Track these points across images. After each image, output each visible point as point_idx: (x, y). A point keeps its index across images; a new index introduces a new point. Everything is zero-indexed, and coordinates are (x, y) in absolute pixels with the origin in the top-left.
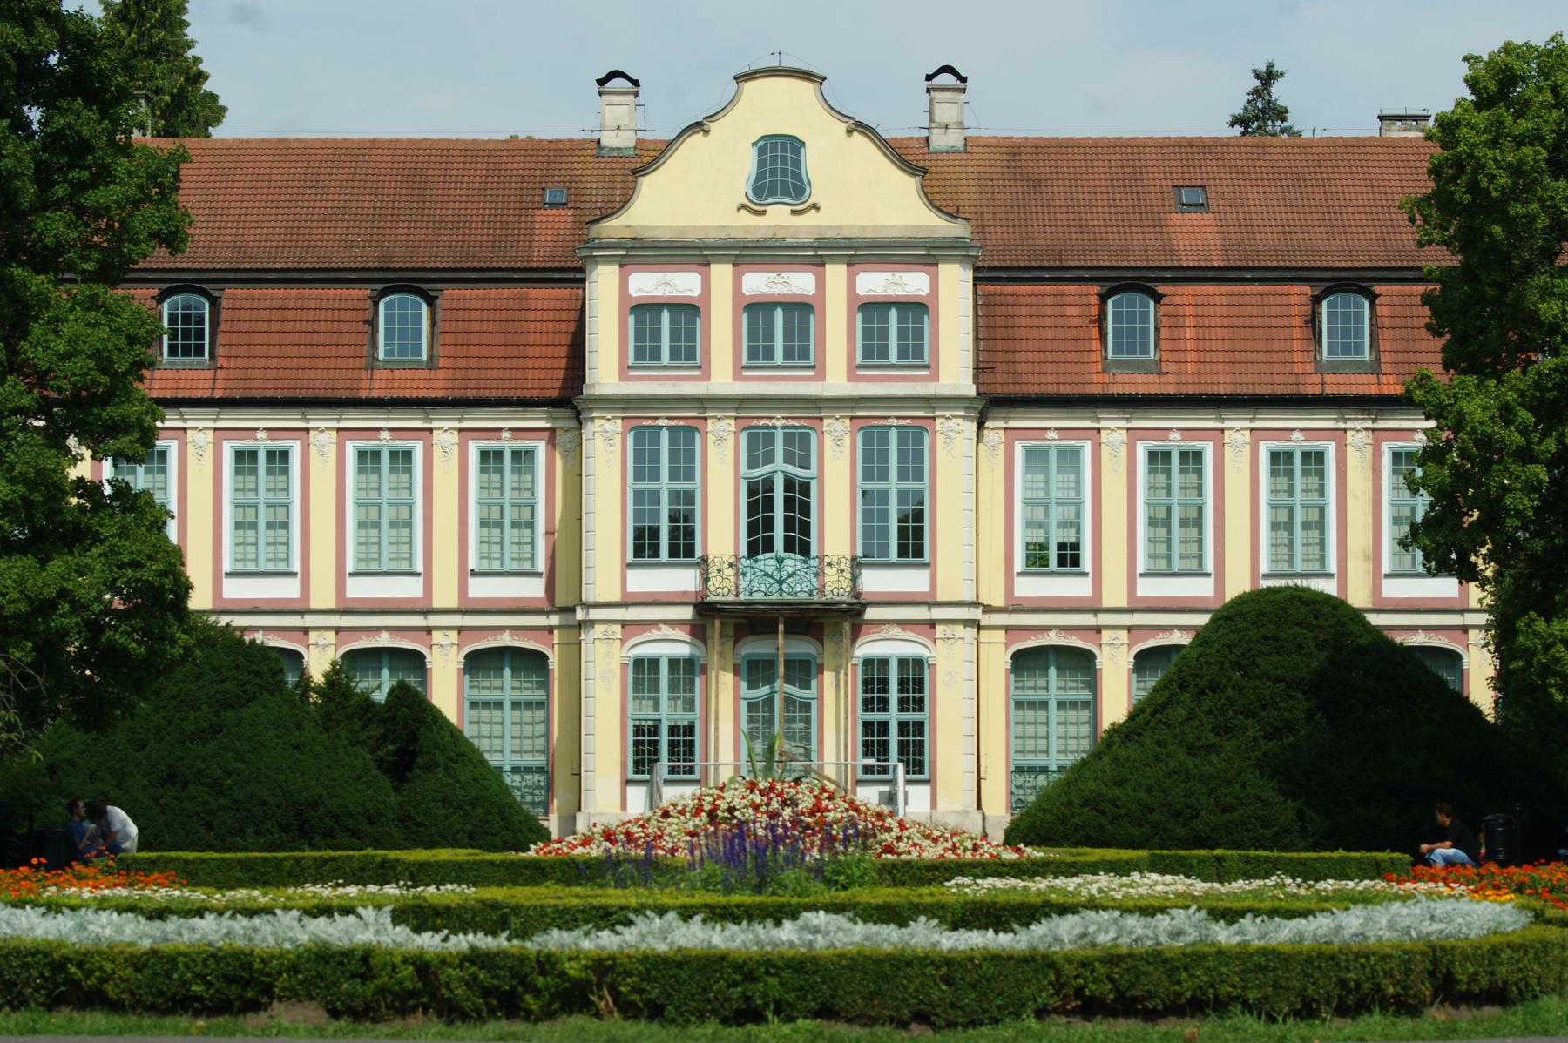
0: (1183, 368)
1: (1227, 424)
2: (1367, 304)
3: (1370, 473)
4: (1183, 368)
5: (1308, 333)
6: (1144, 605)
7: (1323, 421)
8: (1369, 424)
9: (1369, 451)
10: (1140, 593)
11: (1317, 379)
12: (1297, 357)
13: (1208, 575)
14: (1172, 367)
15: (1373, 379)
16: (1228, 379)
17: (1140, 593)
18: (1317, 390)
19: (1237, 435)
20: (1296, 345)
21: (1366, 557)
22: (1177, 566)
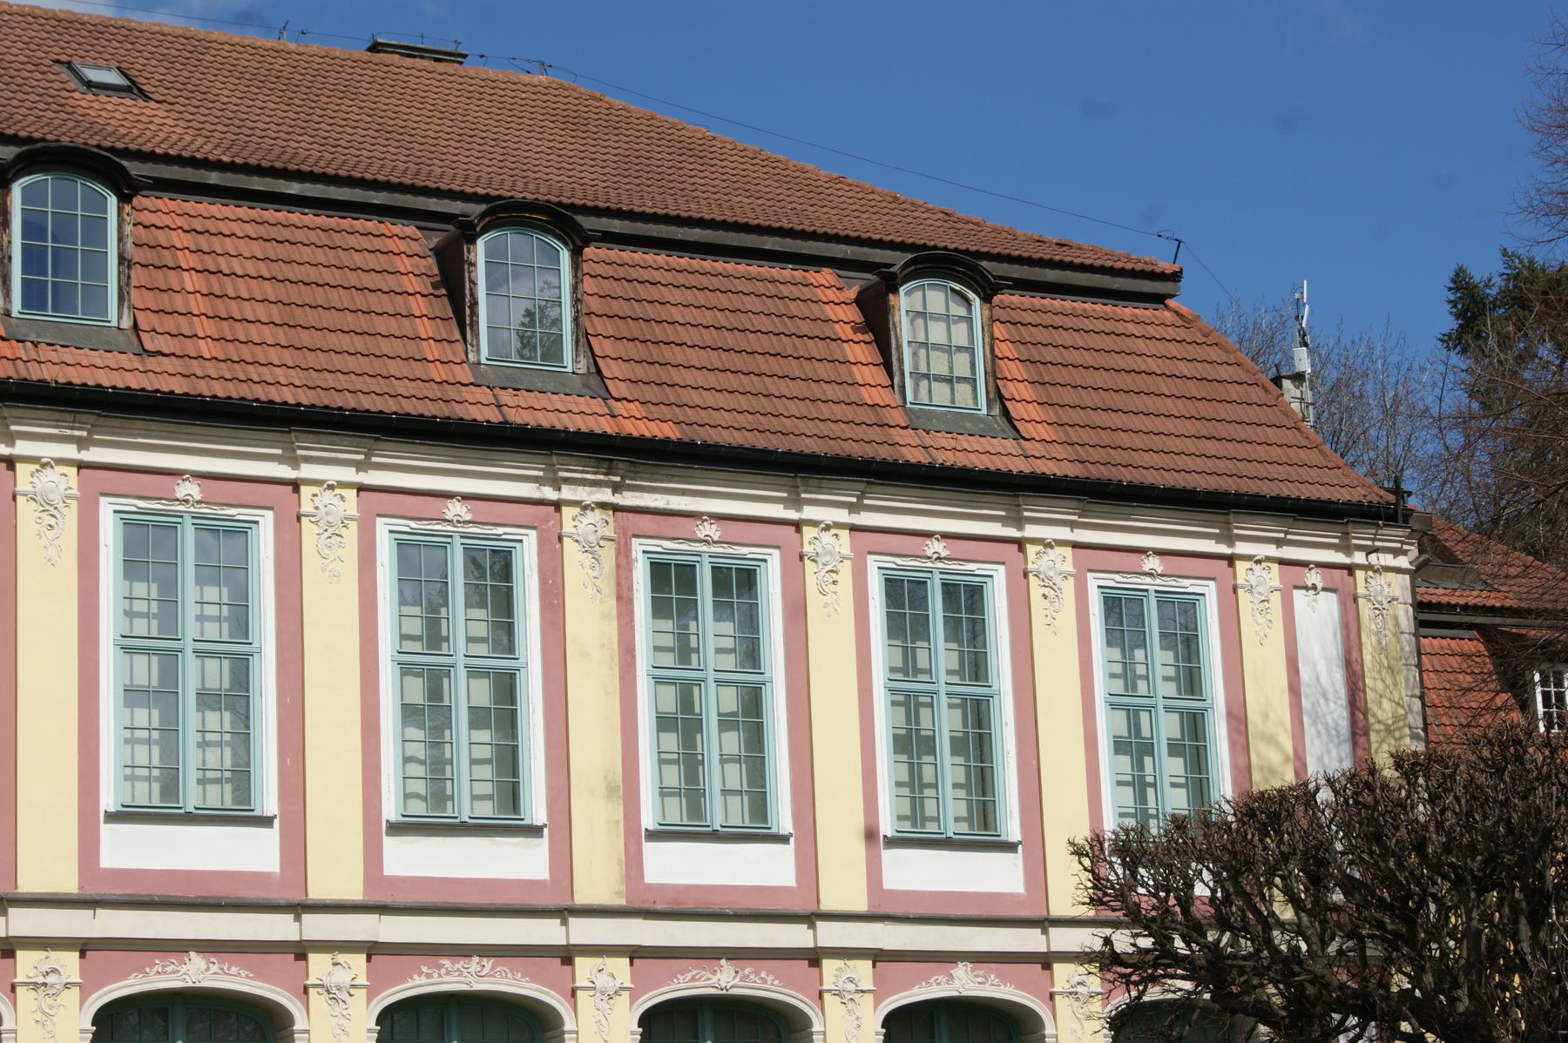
0: (190, 347)
1: (307, 471)
2: (565, 256)
3: (612, 602)
4: (190, 347)
5: (444, 308)
6: (116, 891)
7: (512, 480)
8: (606, 495)
9: (608, 552)
10: (107, 860)
11: (483, 395)
12: (431, 350)
13: (266, 822)
14: (165, 344)
15: (597, 405)
16: (296, 377)
17: (107, 860)
18: (493, 416)
19: (327, 497)
20: (424, 328)
21: (611, 791)
22: (191, 798)
